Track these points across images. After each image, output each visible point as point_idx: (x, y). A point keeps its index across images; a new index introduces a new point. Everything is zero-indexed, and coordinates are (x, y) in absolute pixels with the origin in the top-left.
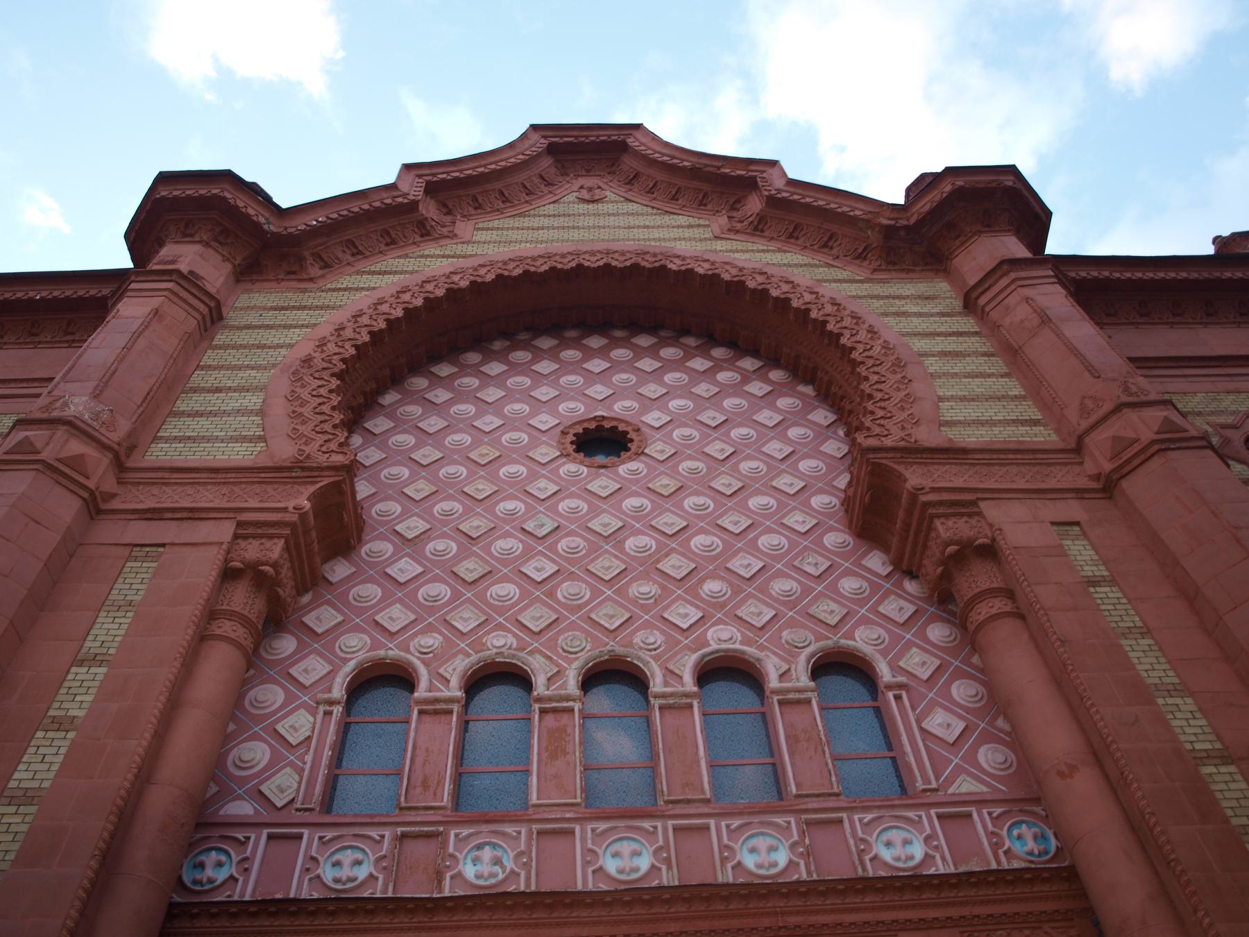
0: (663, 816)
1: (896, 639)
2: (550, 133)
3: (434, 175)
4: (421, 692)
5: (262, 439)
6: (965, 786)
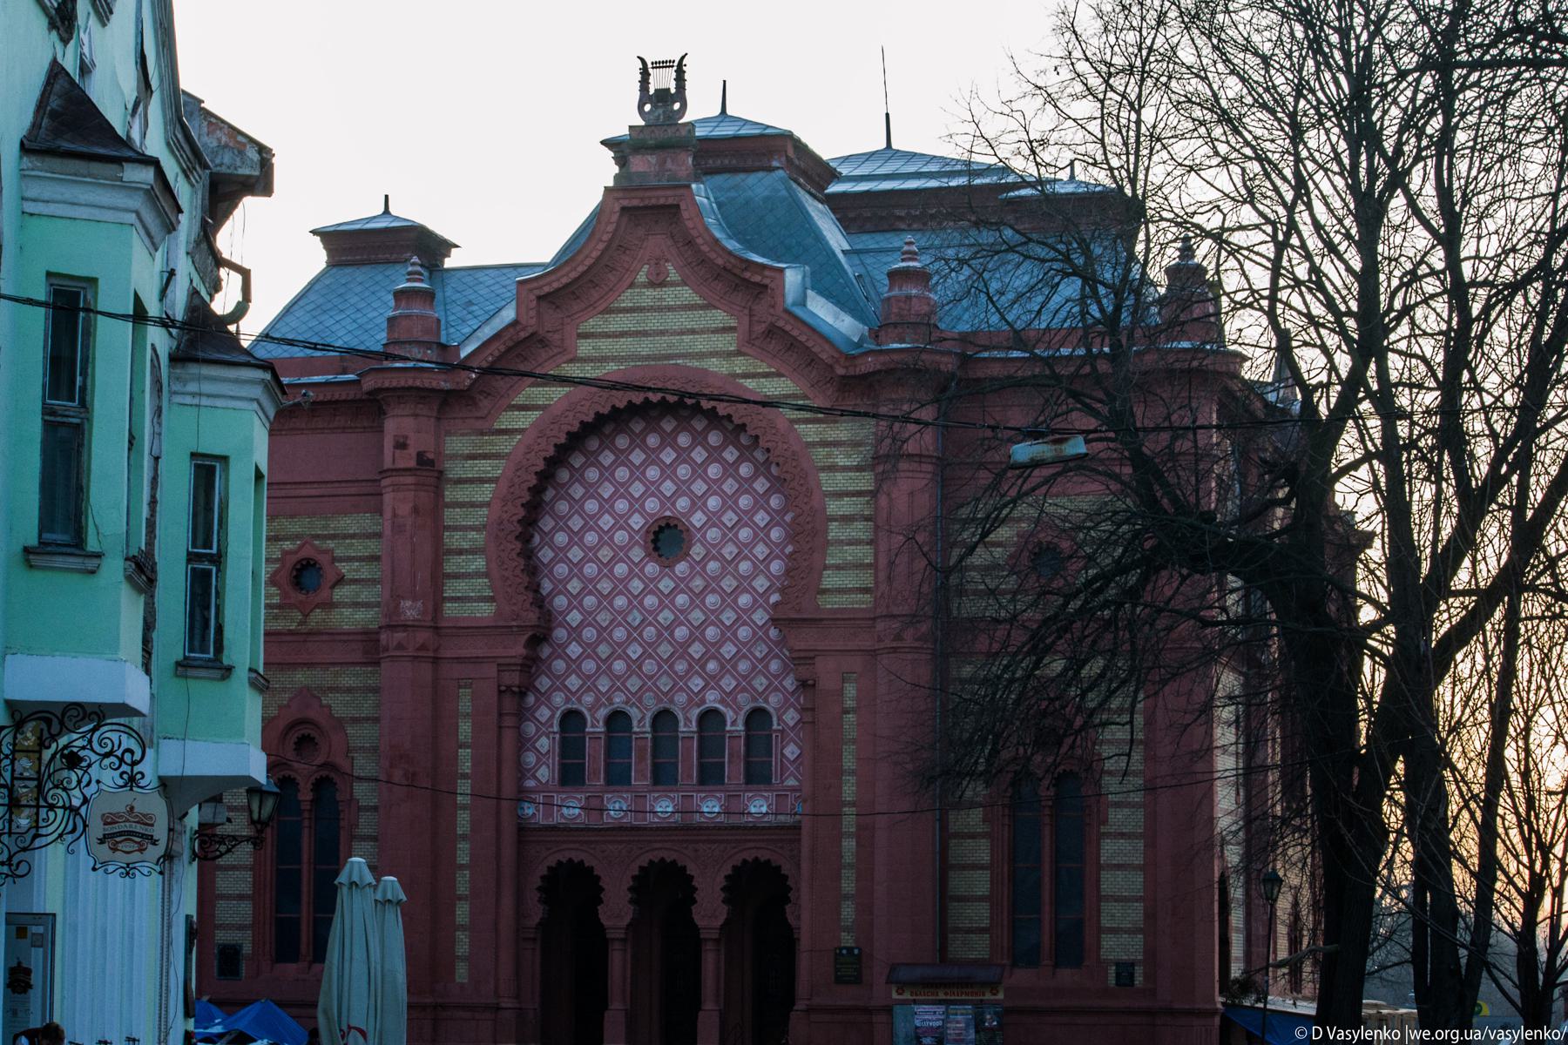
0: (677, 791)
1: (786, 700)
2: (620, 195)
3: (540, 288)
4: (589, 729)
5: (491, 599)
6: (791, 782)
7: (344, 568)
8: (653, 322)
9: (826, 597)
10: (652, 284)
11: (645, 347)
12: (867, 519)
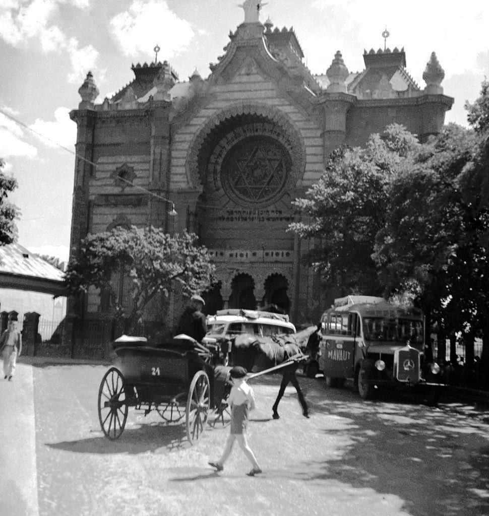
7: (137, 173)
8: (248, 87)
9: (305, 182)
10: (248, 74)
11: (244, 95)
12: (321, 155)
